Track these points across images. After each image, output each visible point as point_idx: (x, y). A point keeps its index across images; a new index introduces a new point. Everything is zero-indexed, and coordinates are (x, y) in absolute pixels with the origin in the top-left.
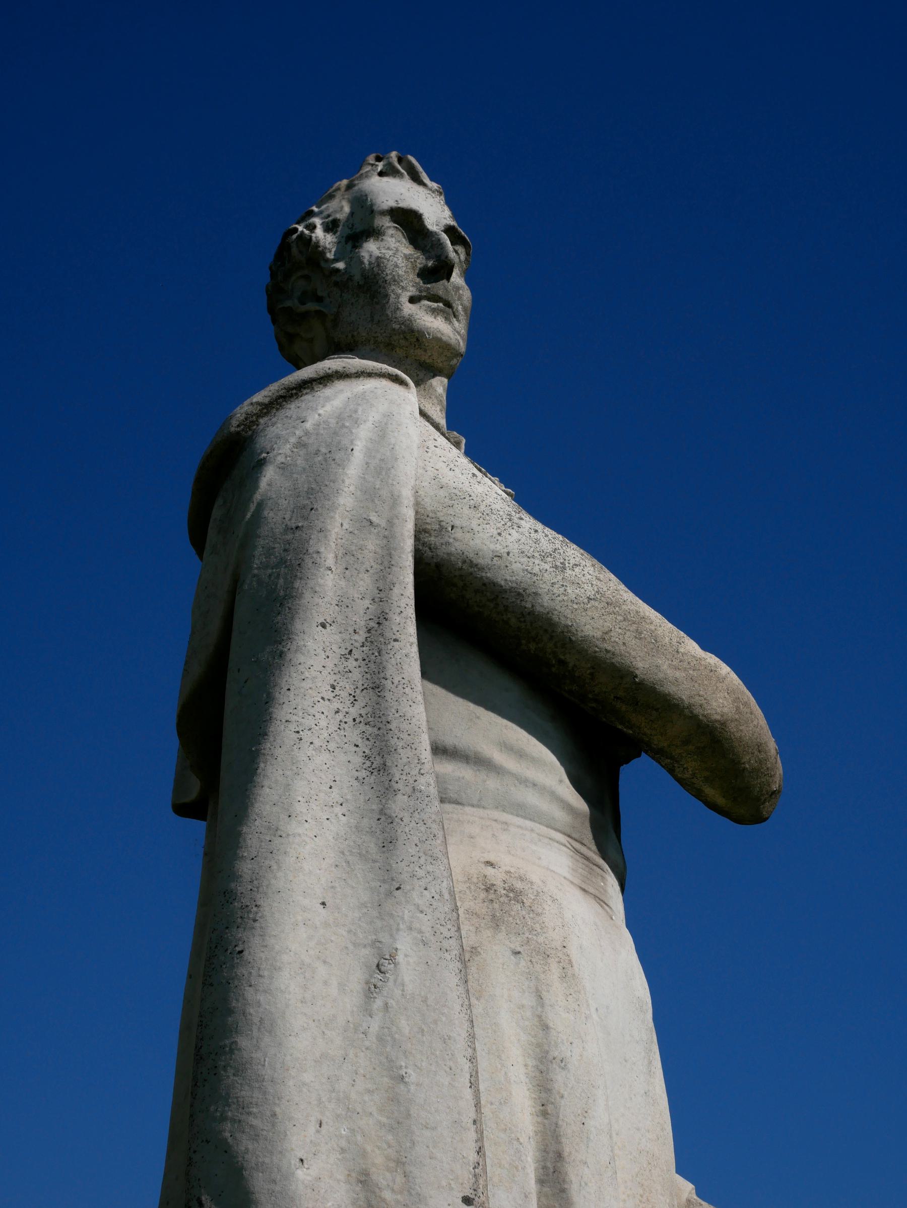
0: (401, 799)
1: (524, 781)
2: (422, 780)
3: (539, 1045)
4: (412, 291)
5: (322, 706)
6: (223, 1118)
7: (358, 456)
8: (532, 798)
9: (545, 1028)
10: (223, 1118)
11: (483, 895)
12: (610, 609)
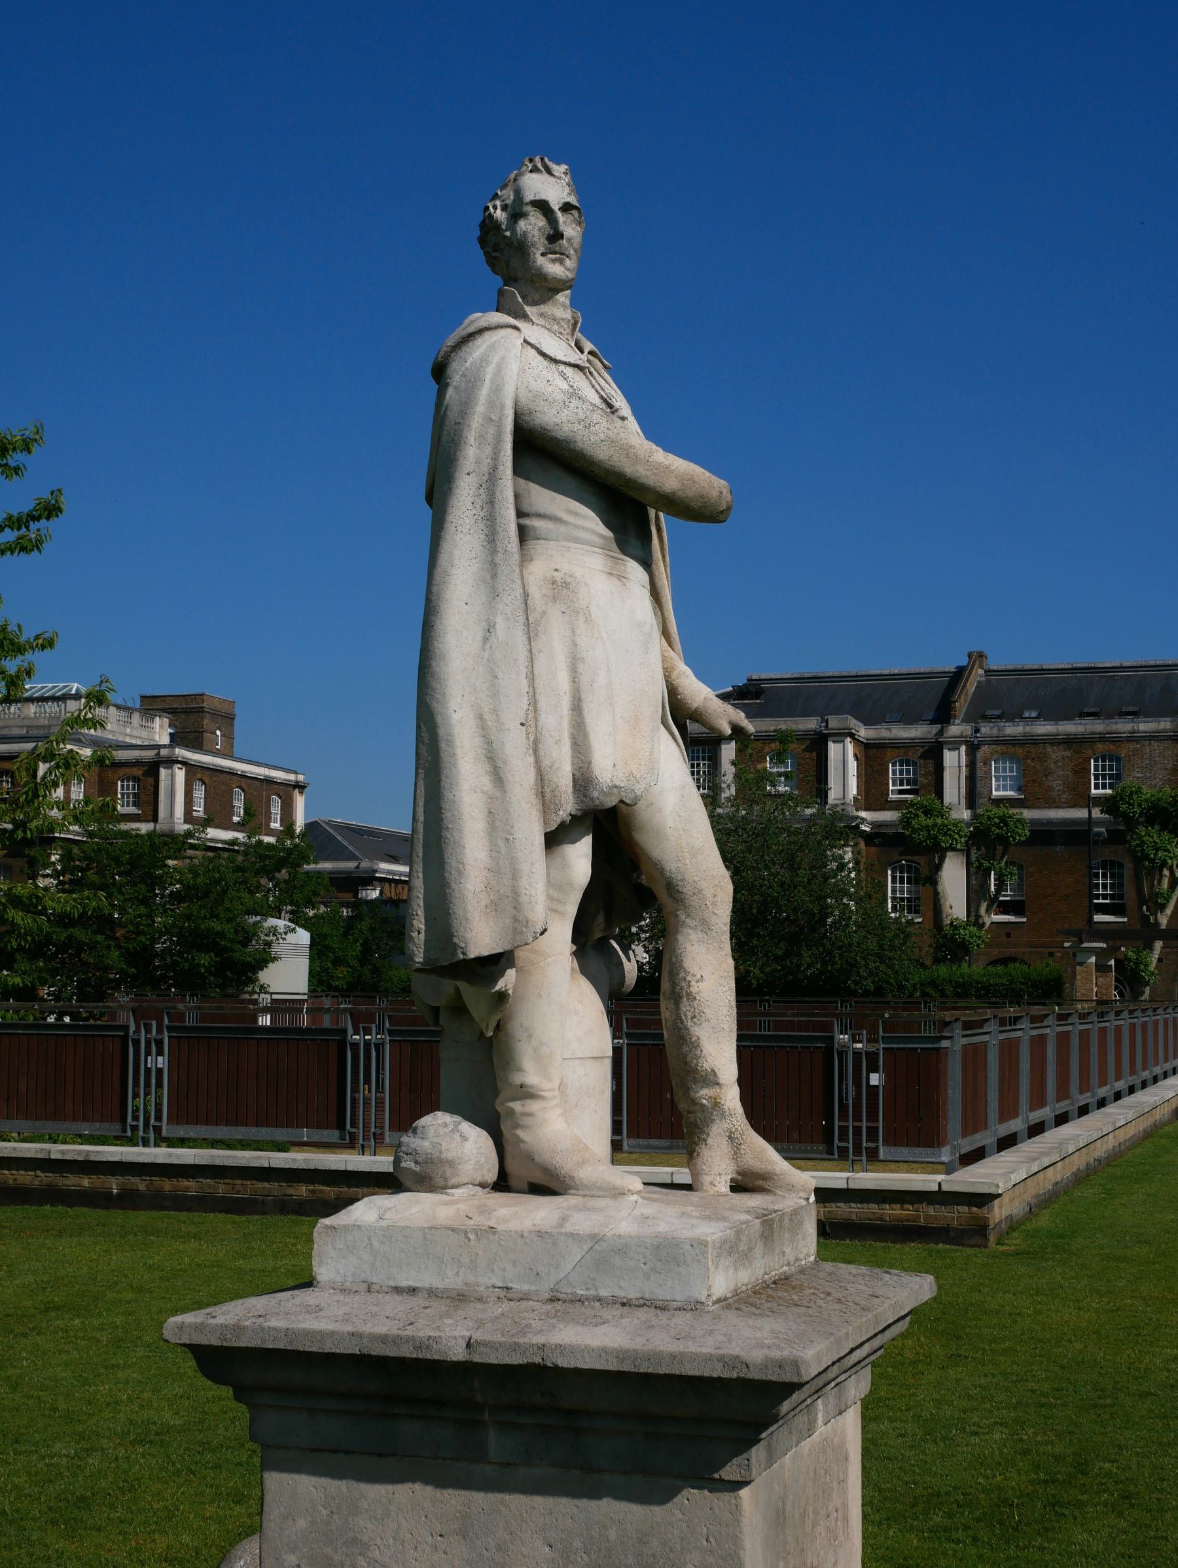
0: (500, 556)
1: (577, 527)
2: (510, 546)
3: (573, 653)
4: (542, 250)
5: (468, 513)
6: (427, 694)
7: (487, 384)
8: (583, 534)
9: (576, 645)
10: (427, 694)
11: (551, 586)
12: (613, 444)
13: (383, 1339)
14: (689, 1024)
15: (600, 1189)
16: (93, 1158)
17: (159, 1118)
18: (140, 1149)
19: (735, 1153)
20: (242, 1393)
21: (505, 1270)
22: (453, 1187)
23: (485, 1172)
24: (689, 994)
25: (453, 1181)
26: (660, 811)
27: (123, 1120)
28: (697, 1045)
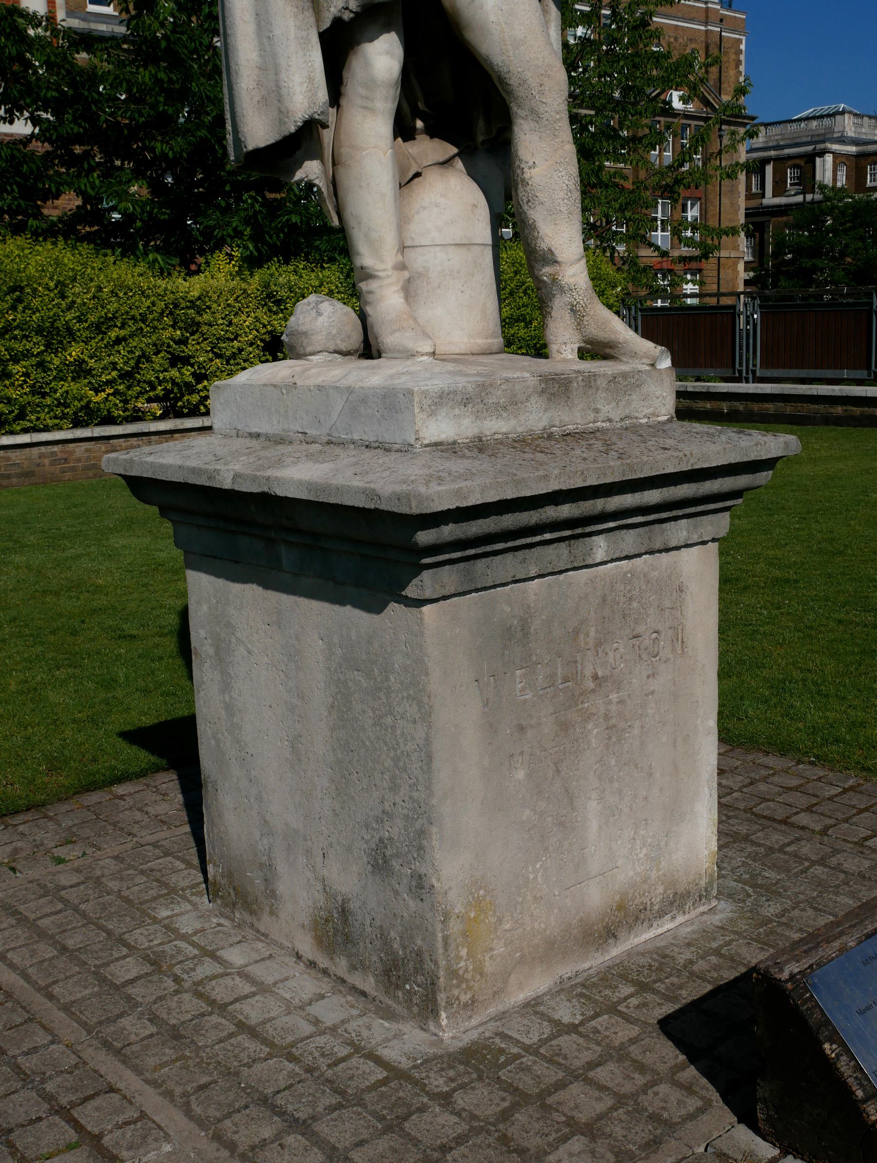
13: (193, 471)
14: (525, 208)
15: (399, 351)
16: (711, 390)
17: (754, 365)
18: (743, 385)
19: (579, 324)
20: (164, 511)
21: (302, 419)
22: (311, 354)
23: (339, 342)
24: (523, 180)
25: (309, 349)
26: (482, 7)
27: (734, 366)
28: (534, 228)
